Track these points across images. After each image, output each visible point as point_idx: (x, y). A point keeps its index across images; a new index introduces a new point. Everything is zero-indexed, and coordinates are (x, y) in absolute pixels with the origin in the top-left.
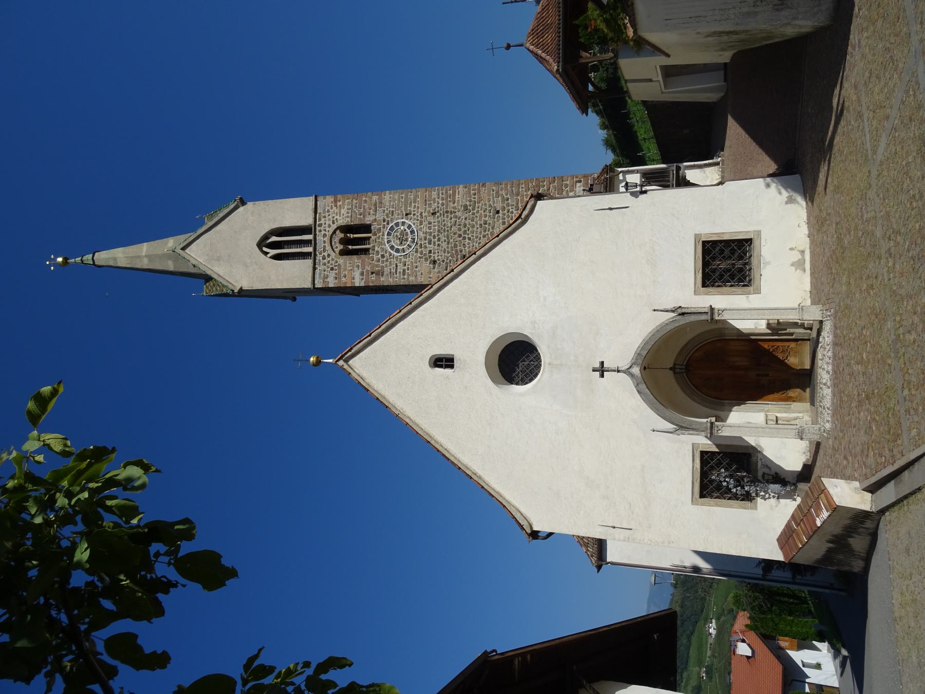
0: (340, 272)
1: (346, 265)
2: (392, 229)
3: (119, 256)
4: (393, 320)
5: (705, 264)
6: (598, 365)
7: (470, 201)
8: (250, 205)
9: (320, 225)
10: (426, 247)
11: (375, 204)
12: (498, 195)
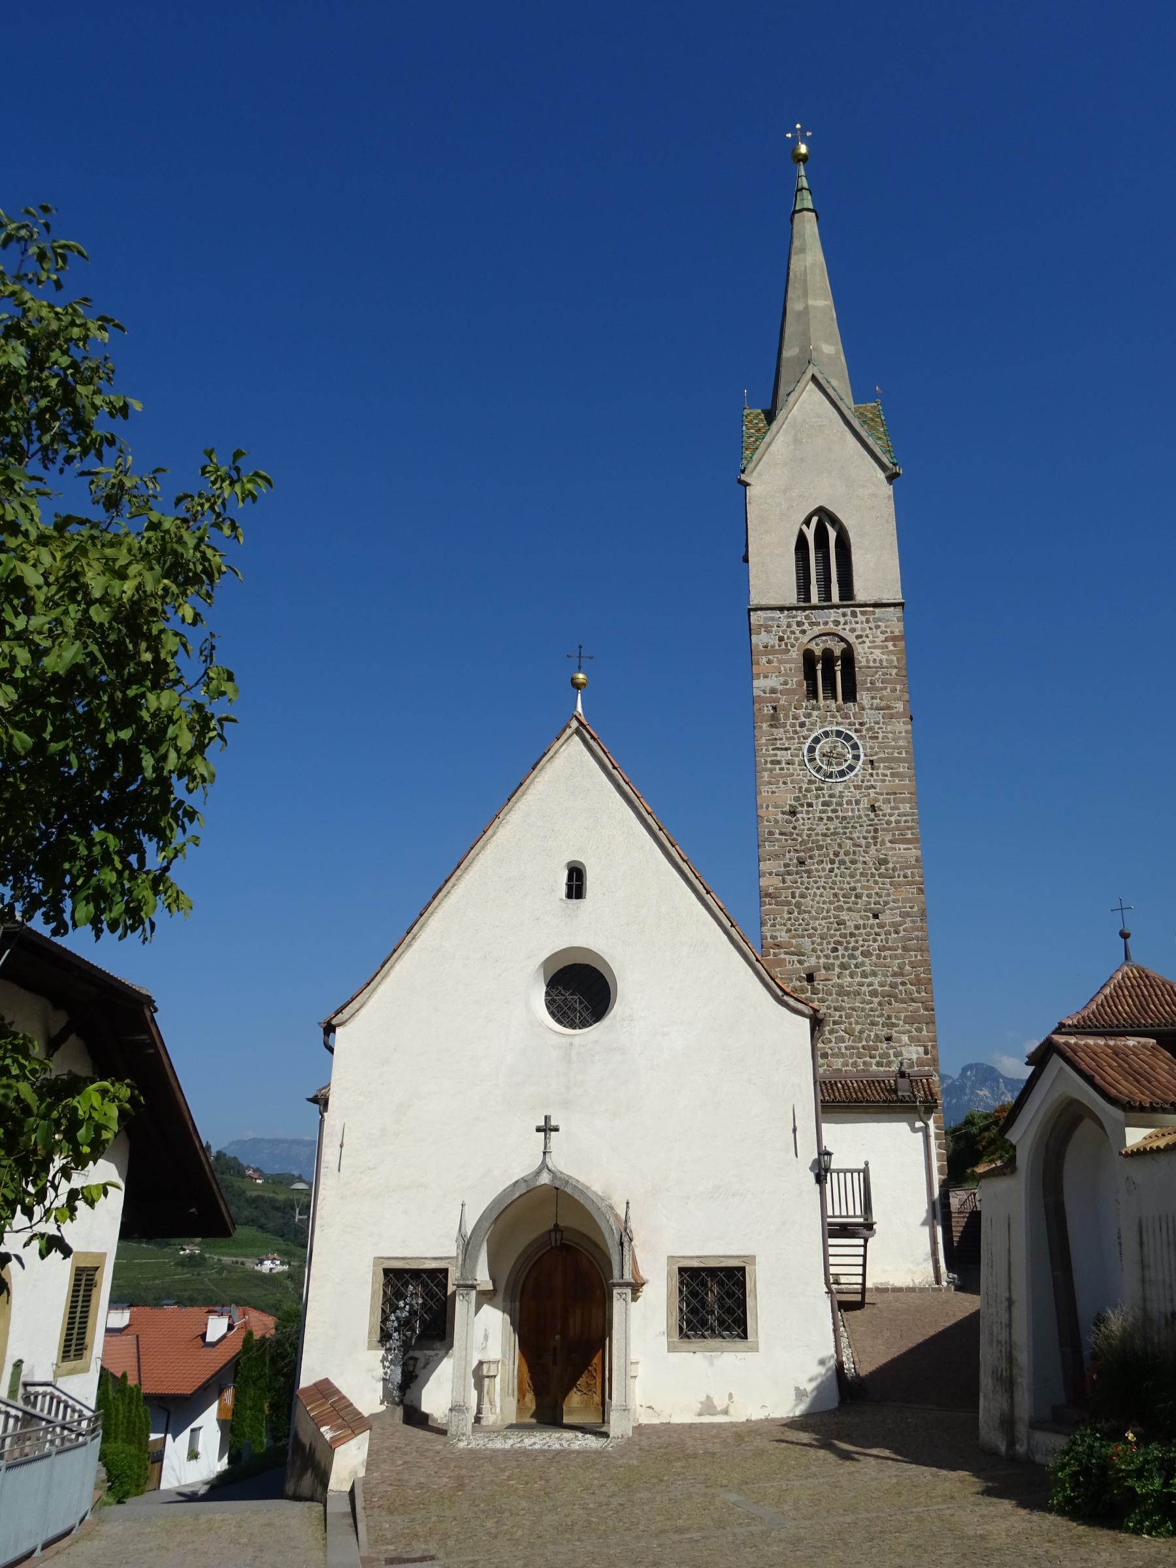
0: (775, 652)
1: (787, 662)
2: (848, 738)
3: (809, 257)
4: (637, 803)
5: (712, 1272)
6: (553, 1123)
7: (894, 869)
8: (888, 490)
9: (854, 614)
10: (817, 797)
11: (889, 708)
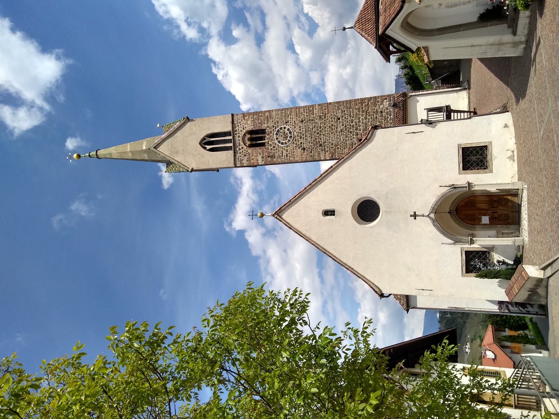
0: (250, 158)
1: (253, 153)
7: (323, 113)
10: (298, 141)
11: (267, 118)
12: (339, 109)
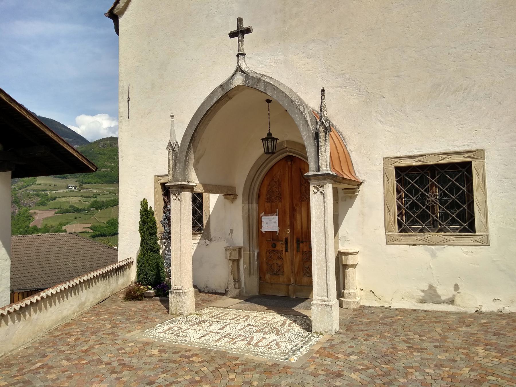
5: (432, 169)
6: (245, 25)
